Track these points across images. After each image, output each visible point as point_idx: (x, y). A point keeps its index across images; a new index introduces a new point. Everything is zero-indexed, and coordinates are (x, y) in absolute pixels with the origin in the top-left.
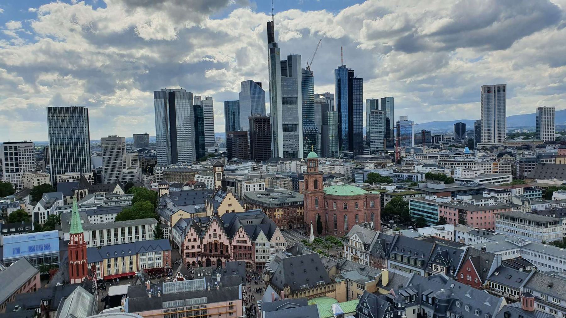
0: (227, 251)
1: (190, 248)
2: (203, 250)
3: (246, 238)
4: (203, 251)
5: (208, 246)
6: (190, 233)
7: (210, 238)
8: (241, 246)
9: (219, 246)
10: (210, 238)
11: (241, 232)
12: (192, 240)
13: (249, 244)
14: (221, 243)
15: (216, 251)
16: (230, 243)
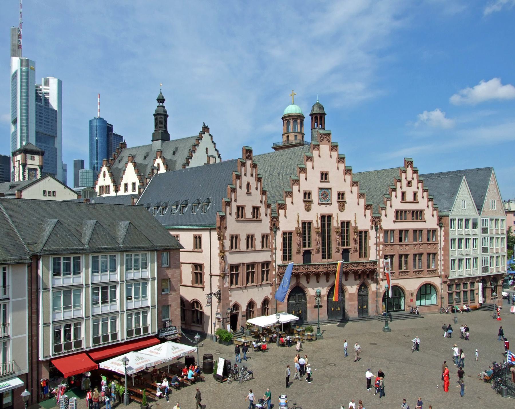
0: (363, 251)
1: (243, 245)
2: (279, 254)
3: (422, 204)
4: (279, 261)
5: (296, 239)
6: (245, 180)
7: (308, 209)
8: (407, 231)
9: (335, 237)
10: (308, 209)
11: (409, 184)
12: (248, 213)
13: (430, 222)
14: (345, 225)
15: (326, 254)
16: (376, 221)
